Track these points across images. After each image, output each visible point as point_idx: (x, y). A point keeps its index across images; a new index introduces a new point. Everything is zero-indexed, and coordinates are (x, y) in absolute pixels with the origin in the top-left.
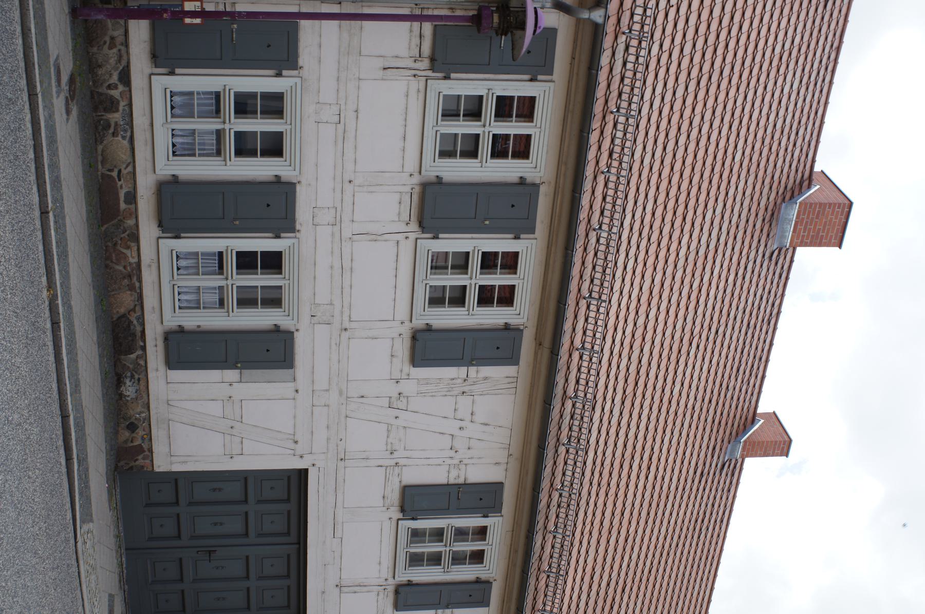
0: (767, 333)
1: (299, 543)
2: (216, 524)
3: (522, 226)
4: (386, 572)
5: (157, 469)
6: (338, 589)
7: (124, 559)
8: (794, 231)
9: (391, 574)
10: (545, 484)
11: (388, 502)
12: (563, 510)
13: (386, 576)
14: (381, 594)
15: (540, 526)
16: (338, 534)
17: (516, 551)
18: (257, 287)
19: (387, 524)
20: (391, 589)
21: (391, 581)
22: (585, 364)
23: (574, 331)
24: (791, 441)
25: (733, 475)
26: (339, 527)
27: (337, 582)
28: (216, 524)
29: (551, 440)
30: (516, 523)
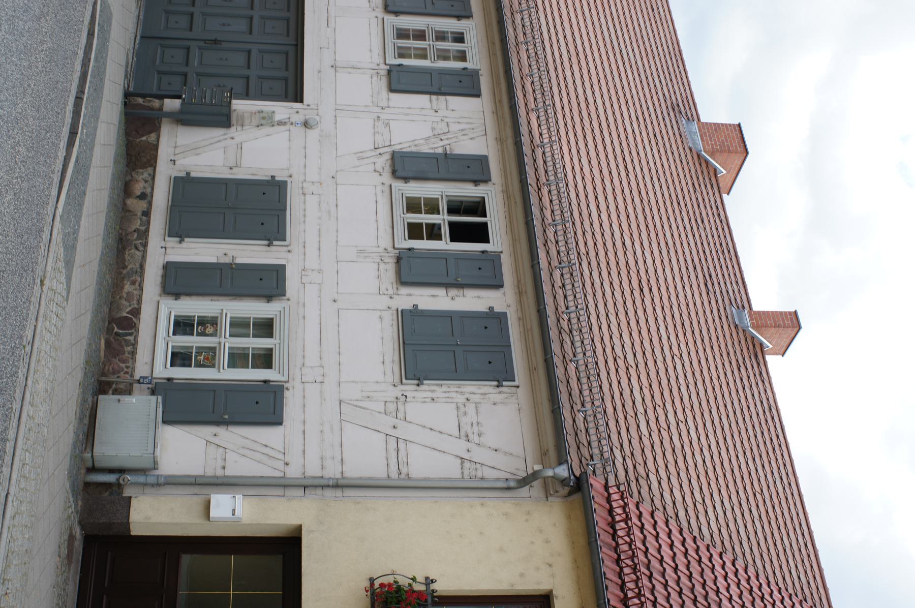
0: (778, 436)
1: (297, 45)
2: (224, 25)
3: (482, 178)
4: (377, 57)
5: (133, 533)
6: (333, 69)
7: (141, 13)
8: (702, 140)
9: (382, 61)
10: (553, 334)
11: (373, 5)
12: (560, 227)
13: (377, 61)
14: (375, 78)
15: (570, 439)
16: (332, 25)
17: (499, 84)
18: (254, 336)
19: (374, 21)
20: (384, 72)
21: (383, 66)
22: (585, 387)
23: (520, 60)
24: (800, 328)
25: (756, 356)
26: (332, 20)
27: (333, 63)
28: (224, 25)
29: (507, 11)
30: (487, 25)
